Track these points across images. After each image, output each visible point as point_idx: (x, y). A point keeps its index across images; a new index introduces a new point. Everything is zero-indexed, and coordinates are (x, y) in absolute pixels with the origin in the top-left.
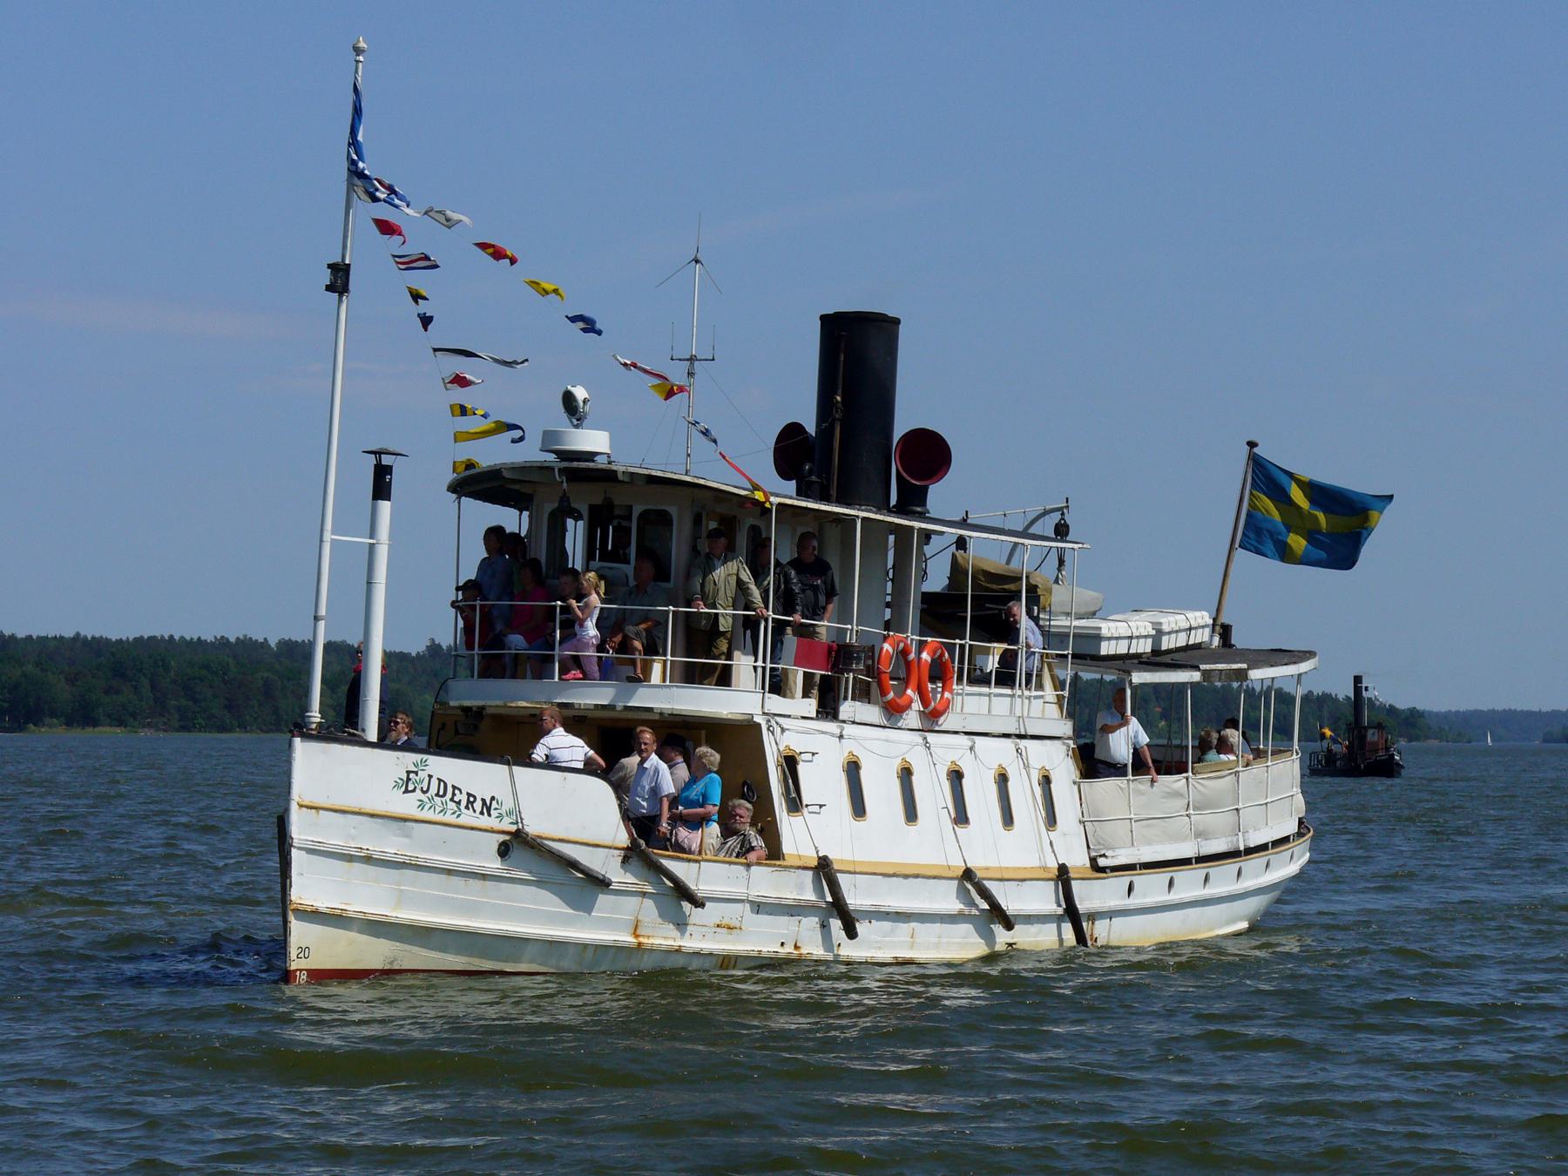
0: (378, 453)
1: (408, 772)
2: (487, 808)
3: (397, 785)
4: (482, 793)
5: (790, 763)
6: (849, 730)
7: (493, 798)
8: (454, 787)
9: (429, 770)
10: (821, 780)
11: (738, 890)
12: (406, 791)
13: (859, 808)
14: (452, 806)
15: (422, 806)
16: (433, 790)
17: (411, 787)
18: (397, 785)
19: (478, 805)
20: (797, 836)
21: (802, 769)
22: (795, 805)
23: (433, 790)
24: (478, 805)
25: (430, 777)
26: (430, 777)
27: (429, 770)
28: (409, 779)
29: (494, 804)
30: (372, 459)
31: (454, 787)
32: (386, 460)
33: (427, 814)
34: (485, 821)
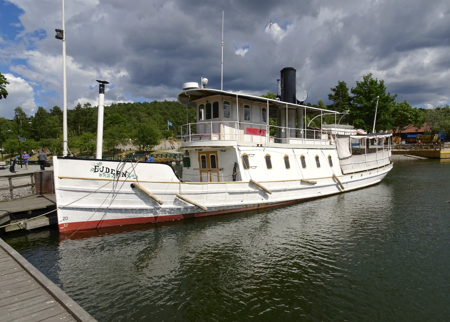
1: (95, 166)
3: (91, 170)
8: (112, 170)
12: (95, 172)
14: (112, 175)
16: (105, 170)
17: (96, 170)
18: (91, 170)
22: (246, 166)
23: (105, 170)
25: (103, 167)
26: (103, 167)
27: (102, 165)
28: (96, 168)
29: (127, 174)
31: (112, 170)
33: (104, 178)
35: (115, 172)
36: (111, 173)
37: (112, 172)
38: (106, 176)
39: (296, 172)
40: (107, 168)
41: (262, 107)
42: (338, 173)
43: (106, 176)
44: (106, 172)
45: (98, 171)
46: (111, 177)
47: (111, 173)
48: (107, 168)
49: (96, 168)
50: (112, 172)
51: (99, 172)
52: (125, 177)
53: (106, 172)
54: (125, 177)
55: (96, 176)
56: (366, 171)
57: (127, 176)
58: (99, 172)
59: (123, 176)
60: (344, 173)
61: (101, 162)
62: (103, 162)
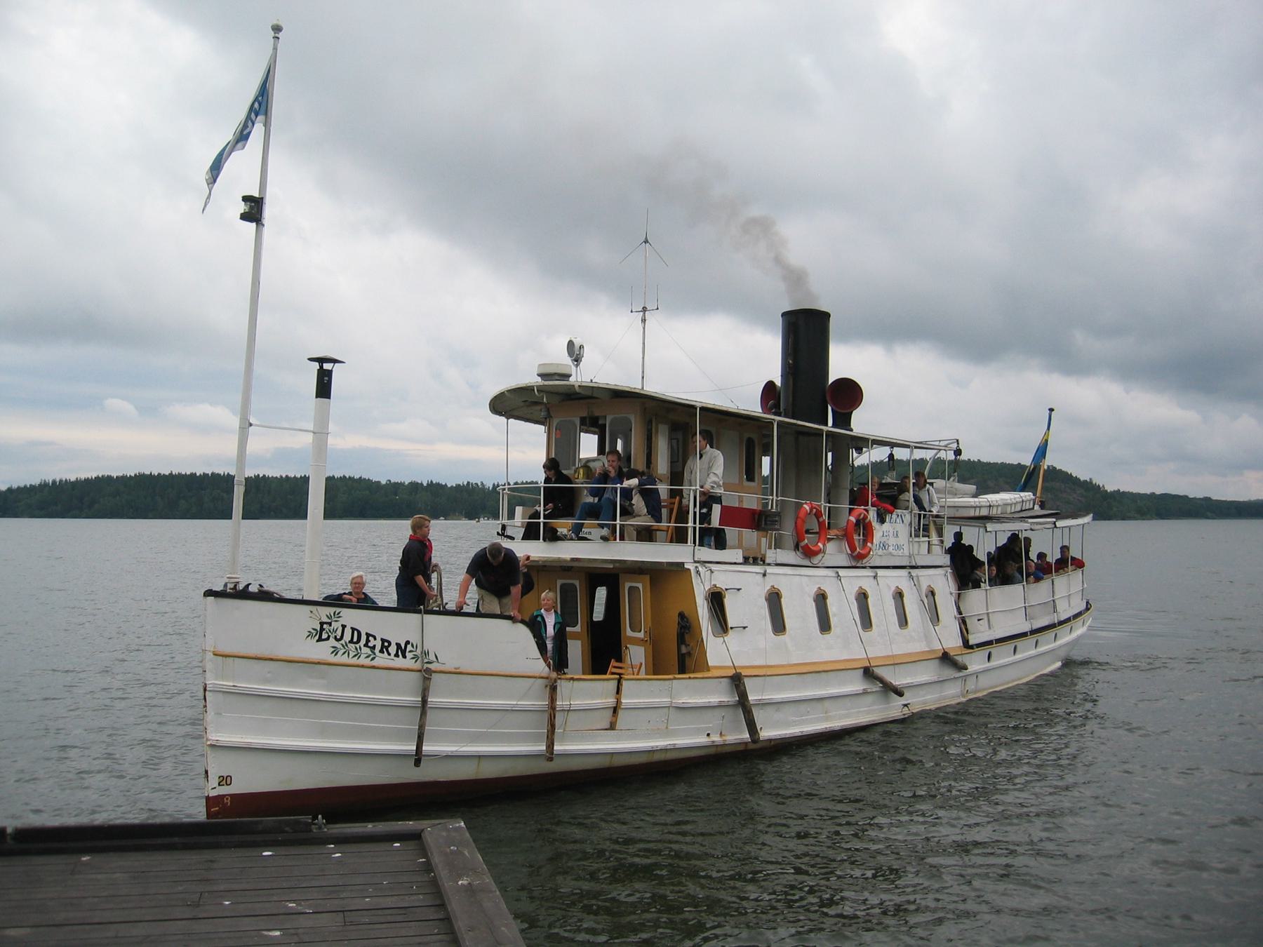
0: (321, 361)
1: (322, 624)
2: (401, 651)
3: (310, 635)
4: (396, 638)
5: (716, 599)
6: (770, 570)
7: (407, 643)
8: (368, 635)
9: (342, 621)
10: (745, 606)
11: (665, 700)
12: (320, 639)
13: (779, 625)
14: (368, 651)
15: (335, 651)
16: (347, 637)
17: (324, 636)
18: (310, 635)
19: (393, 649)
20: (719, 651)
21: (728, 602)
23: (347, 637)
24: (393, 649)
25: (344, 627)
26: (344, 627)
27: (342, 621)
28: (322, 629)
30: (317, 365)
31: (368, 635)
32: (327, 366)
33: (341, 658)
34: (400, 662)
35: (378, 644)
36: (366, 645)
37: (368, 641)
38: (352, 654)
39: (847, 643)
40: (353, 629)
41: (746, 435)
42: (952, 641)
43: (352, 654)
44: (351, 641)
45: (328, 638)
46: (363, 656)
47: (366, 645)
48: (353, 629)
49: (322, 629)
50: (368, 641)
51: (332, 642)
52: (404, 657)
53: (351, 641)
54: (404, 657)
55: (322, 651)
56: (1024, 635)
57: (409, 655)
58: (332, 642)
59: (396, 655)
60: (971, 643)
61: (338, 610)
62: (346, 612)
